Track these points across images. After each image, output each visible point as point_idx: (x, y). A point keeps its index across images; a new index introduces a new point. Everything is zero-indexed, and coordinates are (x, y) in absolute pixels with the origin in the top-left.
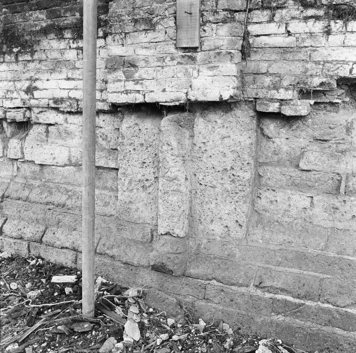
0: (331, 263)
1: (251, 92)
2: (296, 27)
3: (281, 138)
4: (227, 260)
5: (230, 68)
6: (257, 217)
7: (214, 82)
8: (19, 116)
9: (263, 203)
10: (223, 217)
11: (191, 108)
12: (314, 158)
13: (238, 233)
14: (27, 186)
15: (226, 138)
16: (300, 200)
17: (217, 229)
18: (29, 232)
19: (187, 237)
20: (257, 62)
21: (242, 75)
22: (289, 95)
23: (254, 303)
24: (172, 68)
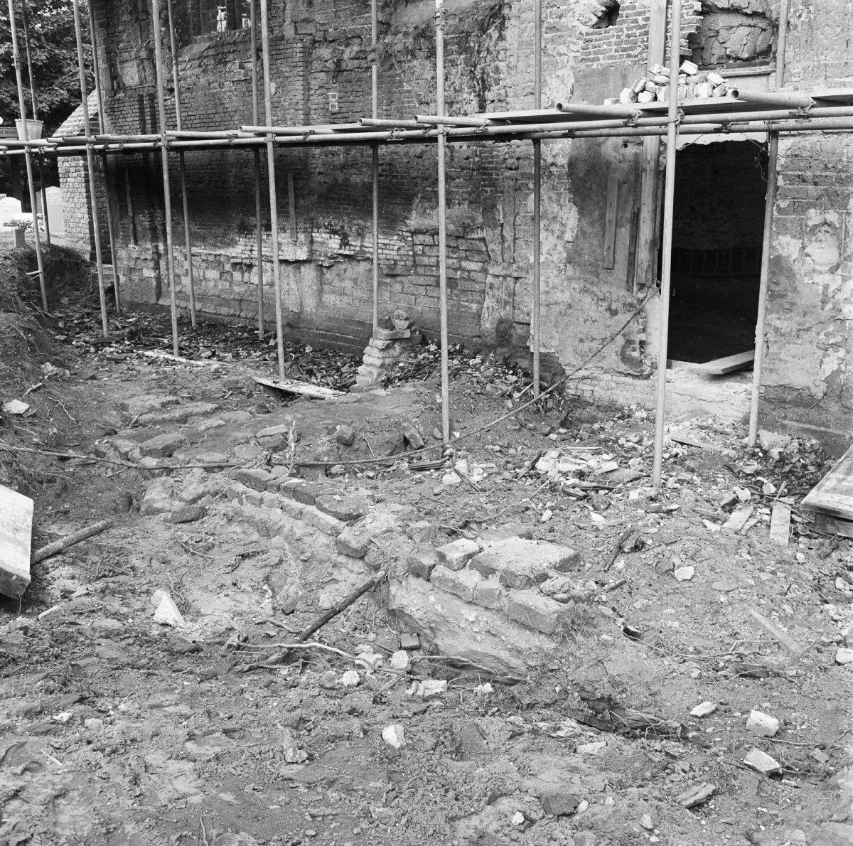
0: (337, 319)
1: (314, 257)
2: (324, 235)
3: (329, 275)
4: (312, 321)
5: (305, 249)
6: (320, 304)
7: (302, 254)
8: (248, 262)
9: (323, 299)
10: (310, 305)
11: (298, 263)
12: (336, 282)
13: (314, 311)
14: (251, 295)
15: (309, 272)
16: (333, 297)
17: (309, 309)
18: (250, 315)
19: (300, 313)
20: (315, 247)
21: (311, 252)
22: (322, 258)
23: (316, 335)
24: (291, 248)
